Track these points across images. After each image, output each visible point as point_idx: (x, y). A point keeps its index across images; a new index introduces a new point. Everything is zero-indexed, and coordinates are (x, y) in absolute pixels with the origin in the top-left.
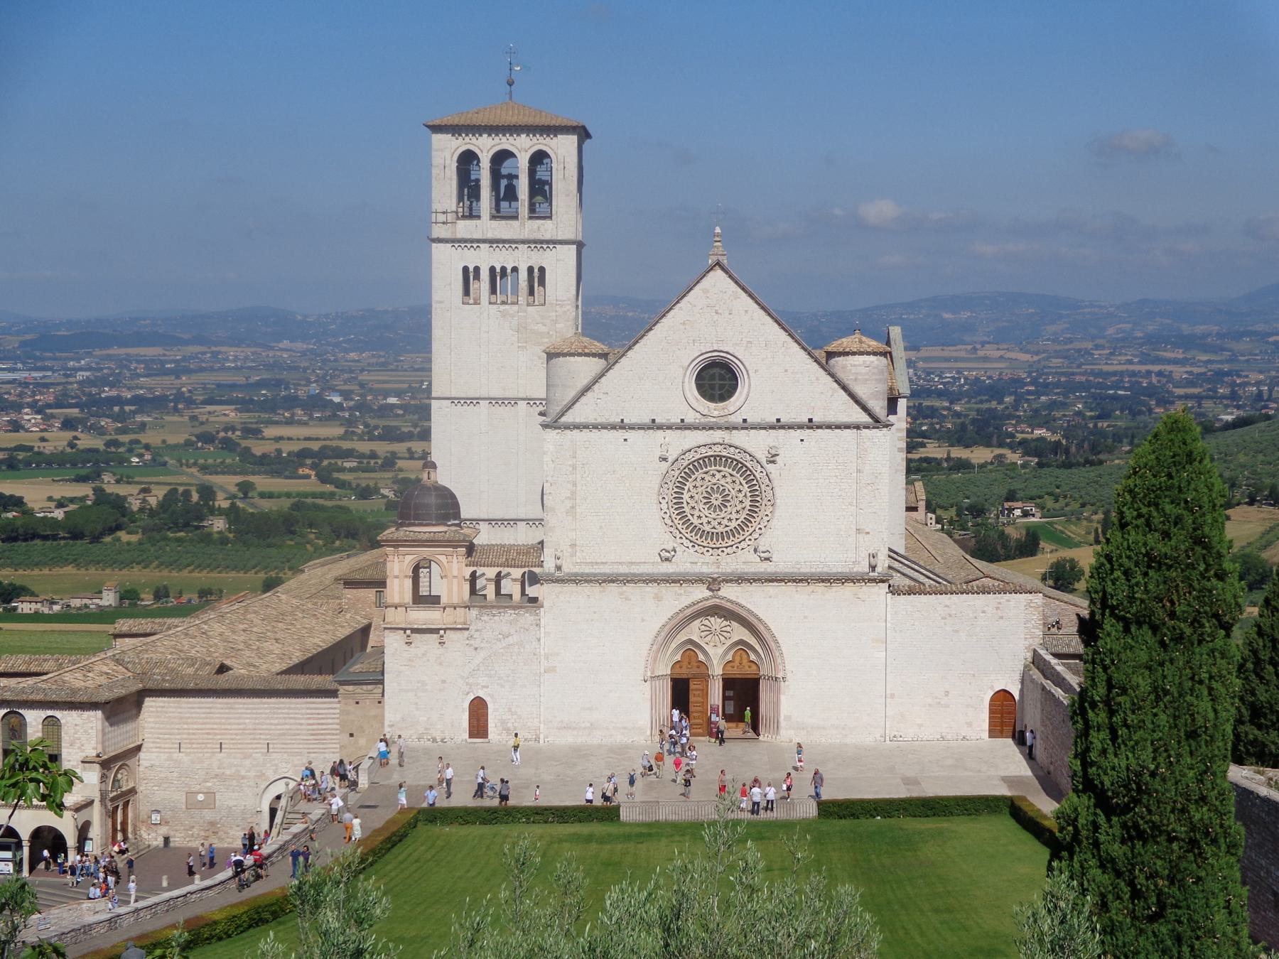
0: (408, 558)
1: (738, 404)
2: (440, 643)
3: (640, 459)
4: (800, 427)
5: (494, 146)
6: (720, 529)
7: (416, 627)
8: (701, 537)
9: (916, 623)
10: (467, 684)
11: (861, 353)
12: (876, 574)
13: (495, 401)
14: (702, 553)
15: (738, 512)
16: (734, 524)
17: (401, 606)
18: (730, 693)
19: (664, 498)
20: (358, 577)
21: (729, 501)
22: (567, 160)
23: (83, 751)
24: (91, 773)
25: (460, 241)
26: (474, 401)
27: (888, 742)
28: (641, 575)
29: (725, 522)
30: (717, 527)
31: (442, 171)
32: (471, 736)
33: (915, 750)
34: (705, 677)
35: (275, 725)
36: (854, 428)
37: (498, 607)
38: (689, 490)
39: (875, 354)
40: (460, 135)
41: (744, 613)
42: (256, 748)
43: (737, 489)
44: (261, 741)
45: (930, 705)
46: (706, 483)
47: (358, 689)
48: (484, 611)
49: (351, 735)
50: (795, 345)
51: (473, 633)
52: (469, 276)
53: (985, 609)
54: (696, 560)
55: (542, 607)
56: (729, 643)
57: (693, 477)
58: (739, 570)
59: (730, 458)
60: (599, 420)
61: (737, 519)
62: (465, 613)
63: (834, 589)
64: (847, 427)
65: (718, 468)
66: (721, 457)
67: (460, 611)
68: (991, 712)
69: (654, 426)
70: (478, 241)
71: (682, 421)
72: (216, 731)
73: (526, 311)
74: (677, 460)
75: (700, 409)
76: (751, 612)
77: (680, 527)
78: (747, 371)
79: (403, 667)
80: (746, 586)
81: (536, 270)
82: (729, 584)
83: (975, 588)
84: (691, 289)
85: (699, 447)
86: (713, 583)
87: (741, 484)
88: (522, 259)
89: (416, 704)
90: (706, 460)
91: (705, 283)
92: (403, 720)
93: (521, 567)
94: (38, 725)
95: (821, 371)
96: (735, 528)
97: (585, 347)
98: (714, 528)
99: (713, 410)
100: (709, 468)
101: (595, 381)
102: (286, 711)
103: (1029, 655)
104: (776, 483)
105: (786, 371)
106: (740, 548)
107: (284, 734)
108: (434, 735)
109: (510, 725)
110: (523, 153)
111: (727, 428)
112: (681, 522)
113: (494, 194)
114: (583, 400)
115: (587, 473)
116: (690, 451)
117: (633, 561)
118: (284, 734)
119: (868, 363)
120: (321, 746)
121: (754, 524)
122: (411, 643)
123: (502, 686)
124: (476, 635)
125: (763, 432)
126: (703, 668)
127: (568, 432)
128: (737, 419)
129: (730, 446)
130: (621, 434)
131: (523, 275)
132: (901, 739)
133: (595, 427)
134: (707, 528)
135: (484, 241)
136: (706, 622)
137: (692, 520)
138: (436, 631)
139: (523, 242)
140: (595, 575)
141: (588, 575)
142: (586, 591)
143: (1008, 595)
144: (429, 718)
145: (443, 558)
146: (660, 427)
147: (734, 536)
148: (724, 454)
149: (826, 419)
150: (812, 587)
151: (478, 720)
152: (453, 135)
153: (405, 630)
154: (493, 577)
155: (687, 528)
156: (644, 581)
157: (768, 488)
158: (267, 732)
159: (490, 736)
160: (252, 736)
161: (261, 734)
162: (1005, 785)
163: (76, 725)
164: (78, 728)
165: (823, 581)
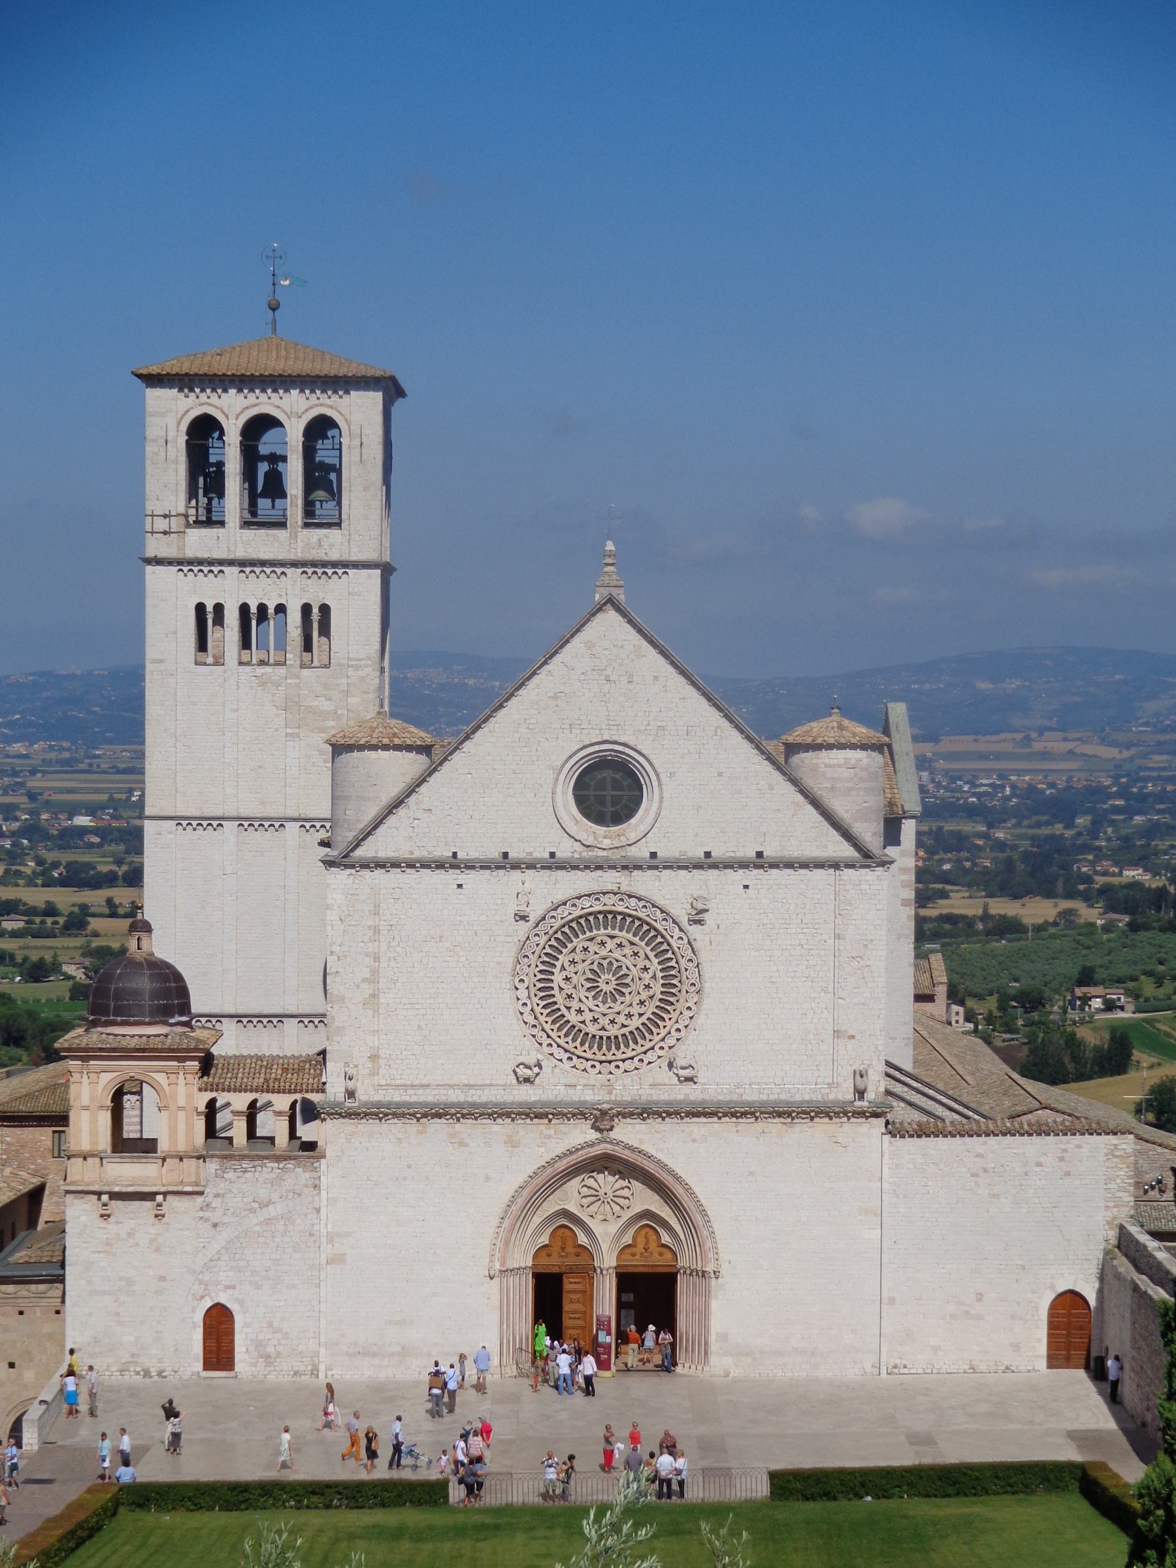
0: (106, 1078)
1: (643, 828)
2: (156, 1216)
3: (483, 918)
4: (744, 865)
5: (247, 408)
6: (613, 1031)
7: (117, 1189)
8: (582, 1044)
9: (930, 1183)
10: (201, 1282)
11: (841, 746)
12: (866, 1104)
13: (247, 822)
14: (584, 1070)
15: (642, 1003)
16: (635, 1023)
17: (93, 1156)
18: (629, 1297)
19: (522, 981)
20: (24, 1108)
21: (627, 985)
22: (365, 432)
25: (190, 562)
26: (214, 822)
27: (884, 1375)
28: (485, 1105)
29: (621, 1019)
30: (608, 1027)
31: (163, 449)
32: (207, 1366)
33: (927, 1389)
34: (587, 1271)
36: (830, 866)
37: (252, 1158)
38: (563, 968)
39: (863, 747)
40: (192, 390)
41: (651, 1167)
43: (641, 965)
45: (953, 1316)
46: (591, 957)
47: (23, 1290)
48: (229, 1164)
49: (12, 1365)
50: (735, 733)
51: (210, 1199)
53: (1042, 1160)
54: (574, 1081)
55: (324, 1157)
56: (627, 1215)
57: (570, 946)
58: (644, 1098)
59: (630, 916)
60: (418, 854)
61: (641, 1015)
62: (198, 1167)
63: (797, 1128)
64: (819, 865)
65: (610, 931)
66: (615, 914)
67: (190, 1164)
68: (1053, 1326)
69: (505, 863)
70: (221, 562)
71: (552, 855)
73: (298, 677)
74: (544, 919)
75: (581, 836)
76: (664, 1167)
77: (547, 1027)
78: (657, 775)
79: (97, 1255)
80: (655, 1123)
81: (315, 610)
82: (628, 1120)
83: (1026, 1127)
84: (567, 642)
85: (579, 898)
86: (602, 1118)
87: (647, 957)
89: (118, 1314)
90: (591, 918)
91: (589, 632)
92: (96, 1340)
93: (290, 1092)
95: (777, 774)
96: (638, 1029)
97: (395, 735)
98: (603, 1029)
99: (602, 837)
100: (595, 932)
101: (411, 790)
103: (1113, 1235)
104: (704, 956)
105: (720, 774)
106: (646, 1062)
108: (147, 1364)
109: (270, 1349)
110: (294, 420)
111: (625, 868)
112: (550, 1020)
113: (246, 485)
114: (391, 821)
115: (398, 939)
116: (565, 904)
117: (472, 1082)
119: (853, 762)
121: (668, 1023)
122: (109, 1216)
123: (258, 1287)
124: (216, 1203)
125: (683, 873)
126: (585, 1256)
127: (366, 873)
128: (641, 852)
129: (630, 896)
131: (294, 617)
132: (906, 1371)
133: (411, 865)
134: (592, 1029)
135: (231, 563)
136: (591, 1182)
137: (568, 1016)
138: (149, 1196)
139: (294, 564)
140: (409, 1105)
141: (399, 1105)
142: (394, 1131)
143: (1078, 1137)
144: (137, 1339)
145: (161, 1078)
146: (516, 866)
147: (636, 1043)
148: (620, 909)
149: (786, 853)
150: (760, 1125)
151: (218, 1342)
152: (181, 390)
153: (99, 1194)
154: (244, 1108)
155: (559, 1029)
156: (490, 1115)
157: (690, 964)
159: (239, 1367)
162: (1073, 1445)
165: (780, 1115)
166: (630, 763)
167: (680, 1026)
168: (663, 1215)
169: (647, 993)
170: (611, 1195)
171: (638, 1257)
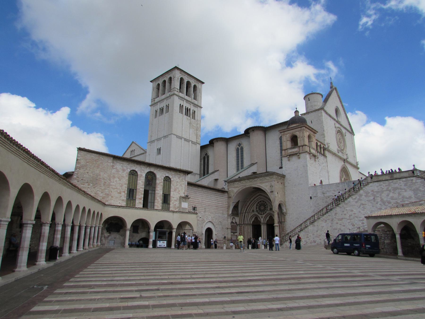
13: (186, 140)
16: (343, 148)
23: (179, 194)
24: (185, 203)
26: (181, 138)
35: (207, 202)
42: (202, 210)
44: (203, 207)
52: (181, 107)
72: (191, 201)
88: (192, 108)
94: (162, 179)
102: (209, 197)
107: (209, 205)
118: (209, 205)
120: (218, 211)
130: (329, 118)
139: (192, 103)
158: (205, 204)
160: (201, 205)
161: (203, 204)
163: (177, 182)
164: (178, 183)
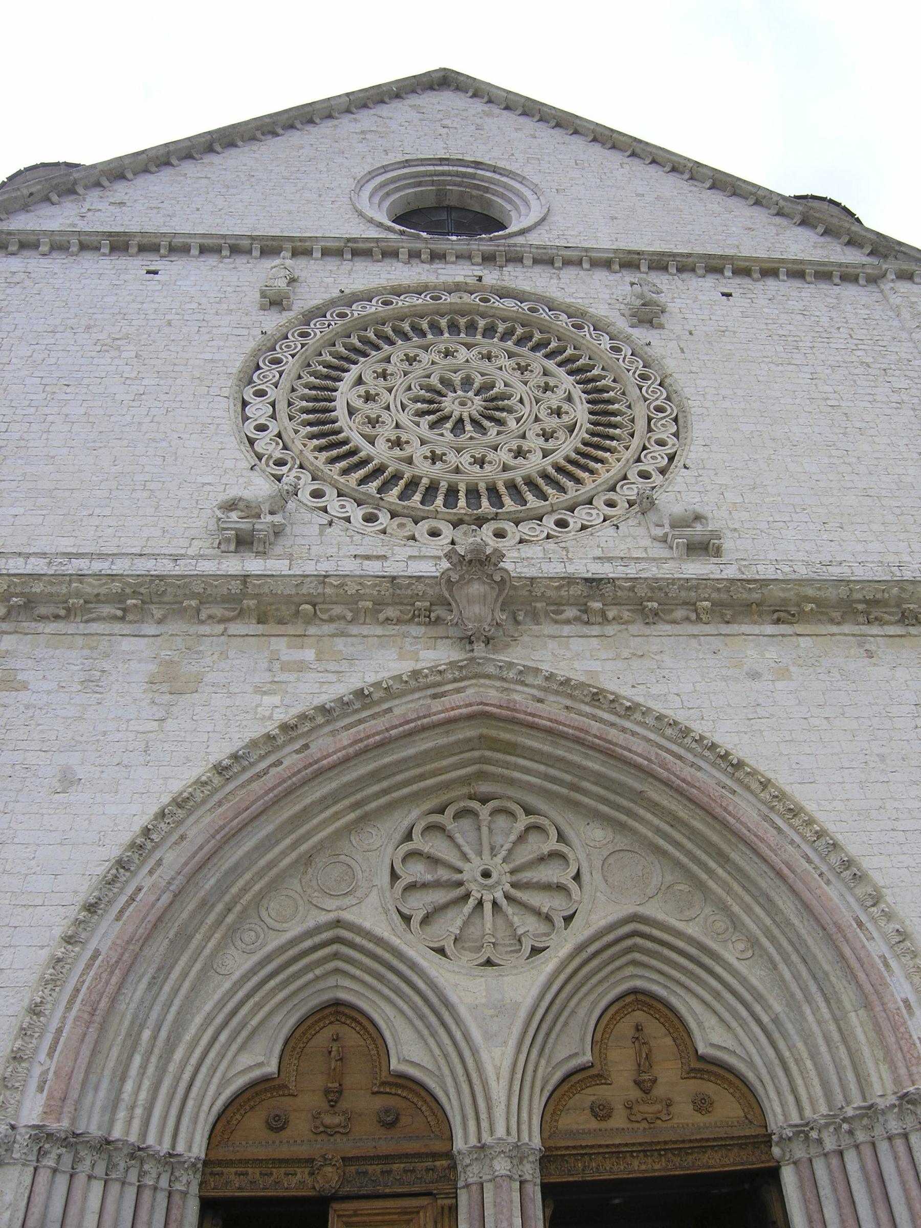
15: (547, 436)
16: (534, 463)
21: (510, 410)
82: (548, 629)
125: (600, 275)
136: (436, 846)
156: (120, 598)
166: (487, 190)
167: (648, 465)
168: (691, 929)
169: (558, 420)
170: (507, 878)
171: (618, 1121)
